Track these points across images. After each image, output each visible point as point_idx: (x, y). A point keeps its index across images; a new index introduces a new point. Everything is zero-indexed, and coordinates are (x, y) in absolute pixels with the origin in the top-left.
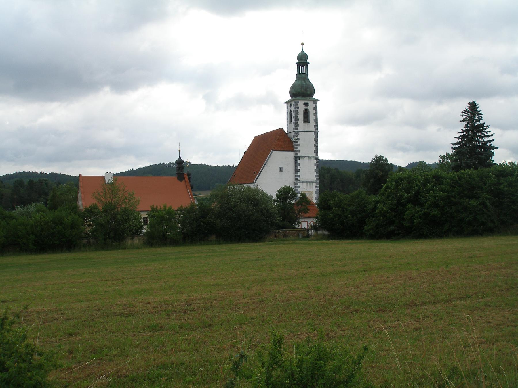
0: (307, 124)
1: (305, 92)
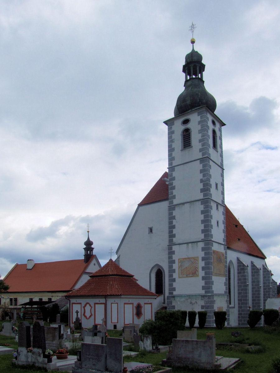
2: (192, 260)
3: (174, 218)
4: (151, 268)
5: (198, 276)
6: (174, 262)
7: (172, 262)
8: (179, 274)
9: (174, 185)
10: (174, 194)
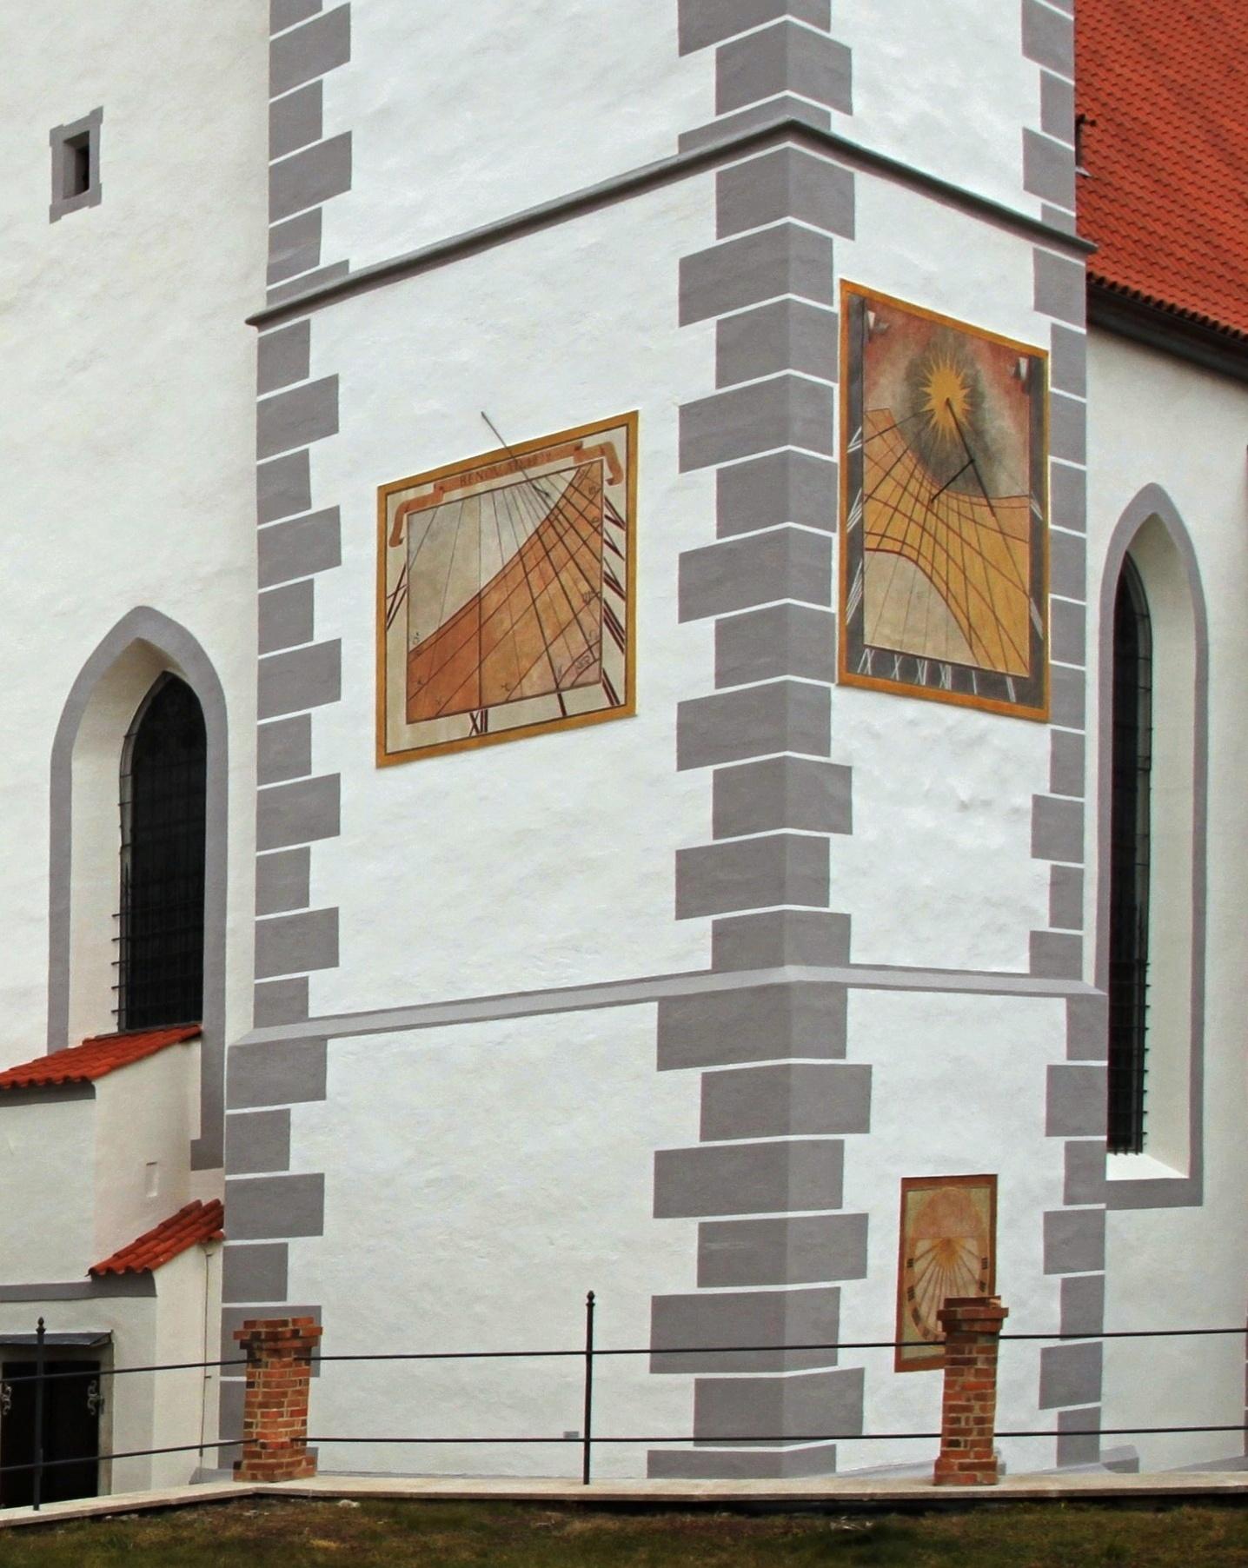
5: (620, 706)
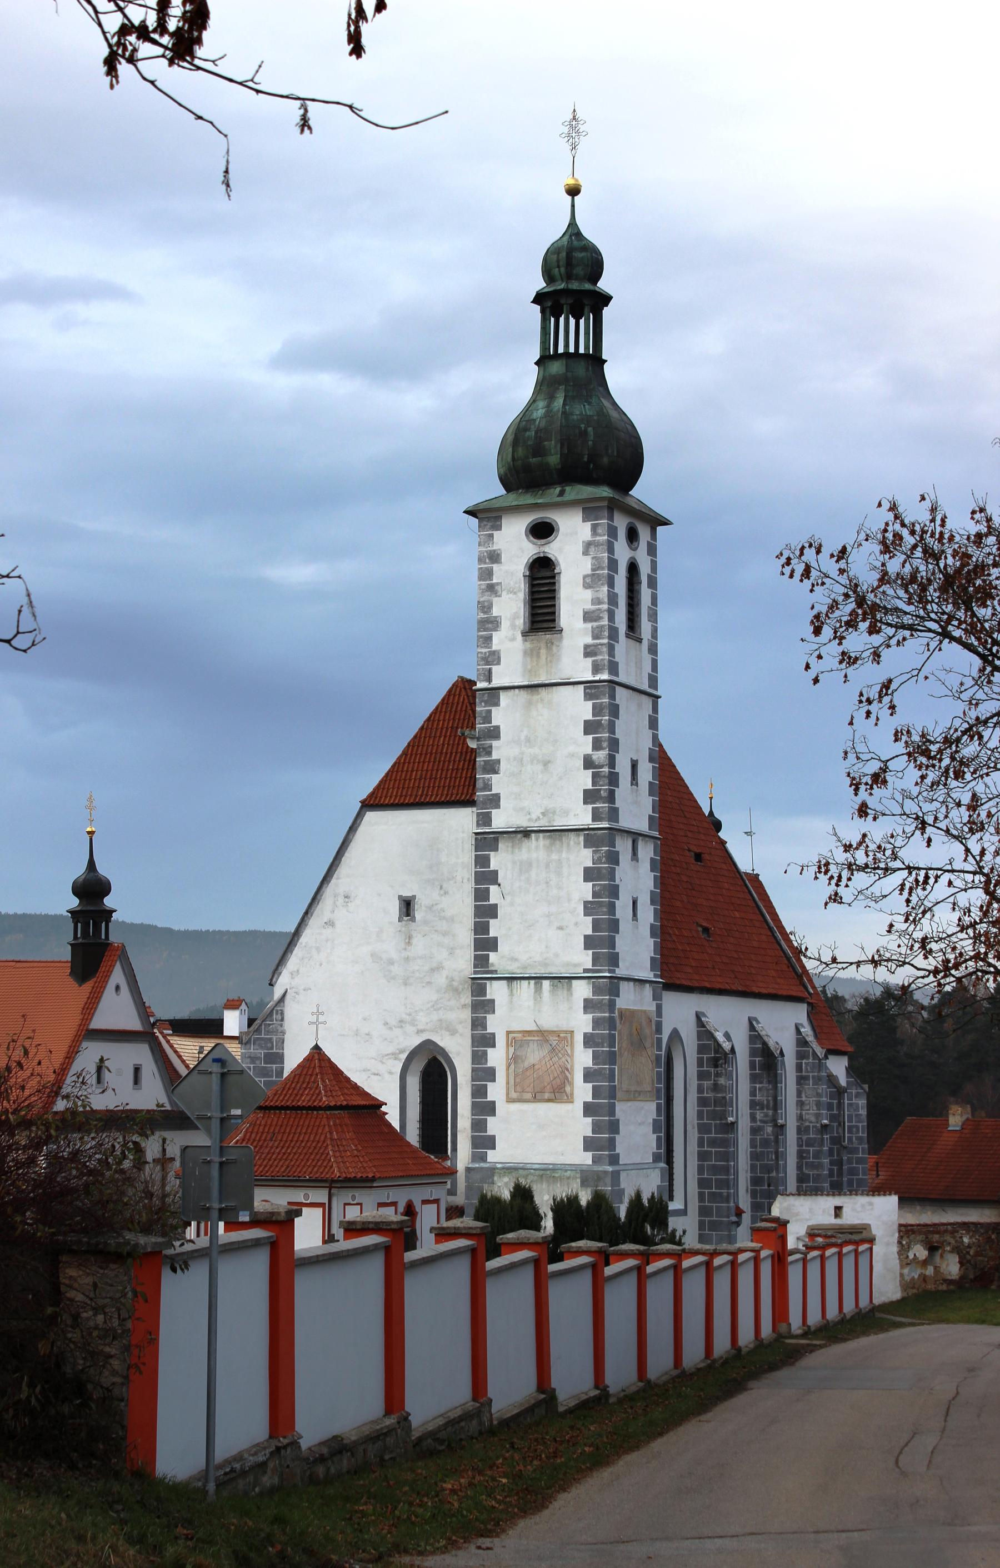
0: (543, 645)
1: (533, 460)
2: (554, 1040)
3: (493, 878)
4: (407, 1053)
5: (570, 1099)
6: (489, 1041)
7: (483, 1041)
8: (508, 1089)
9: (495, 756)
10: (493, 792)
